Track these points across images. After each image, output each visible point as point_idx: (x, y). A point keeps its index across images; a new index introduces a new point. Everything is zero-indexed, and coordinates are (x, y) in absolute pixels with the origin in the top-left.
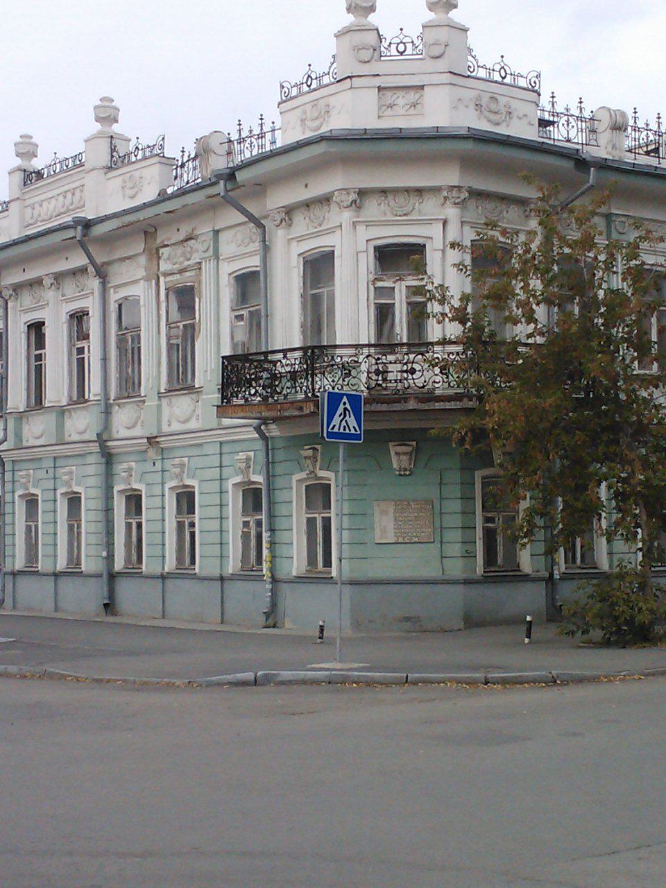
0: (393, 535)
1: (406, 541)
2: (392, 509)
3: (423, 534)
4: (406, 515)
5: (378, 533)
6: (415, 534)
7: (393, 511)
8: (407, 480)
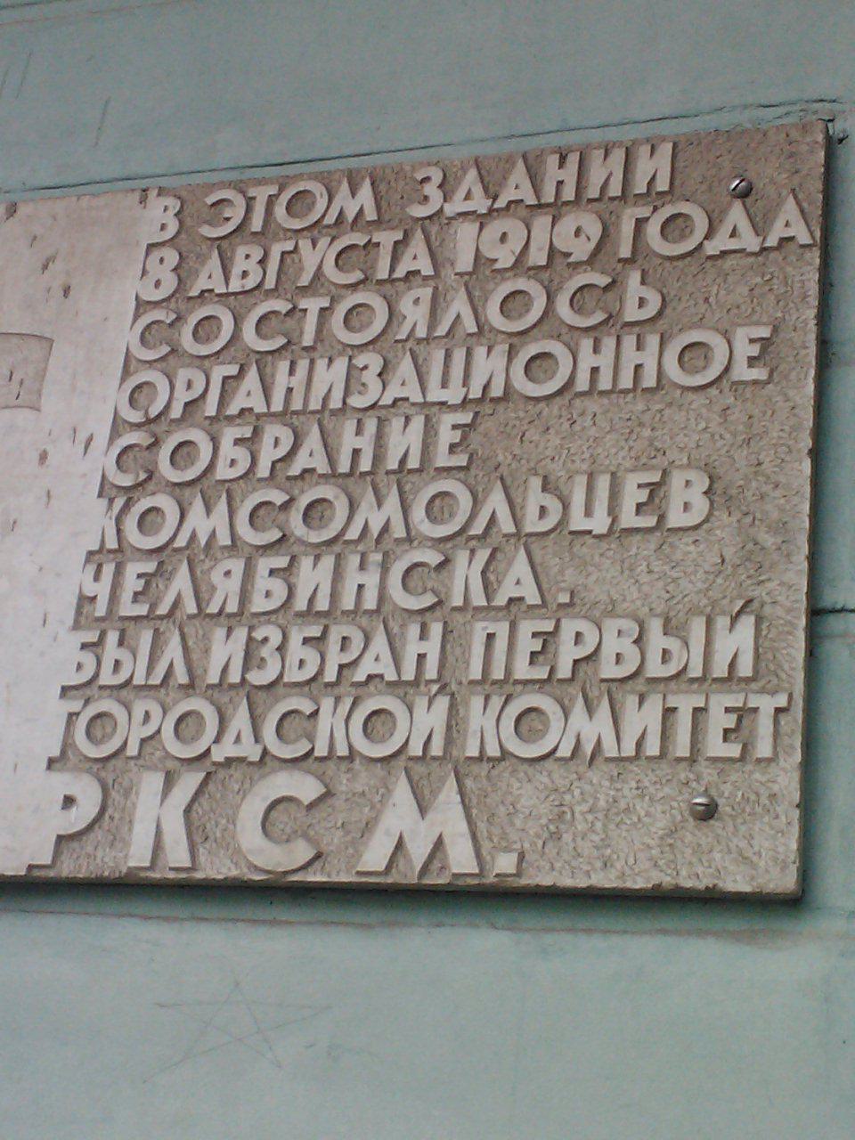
4: (330, 376)
7: (125, 336)
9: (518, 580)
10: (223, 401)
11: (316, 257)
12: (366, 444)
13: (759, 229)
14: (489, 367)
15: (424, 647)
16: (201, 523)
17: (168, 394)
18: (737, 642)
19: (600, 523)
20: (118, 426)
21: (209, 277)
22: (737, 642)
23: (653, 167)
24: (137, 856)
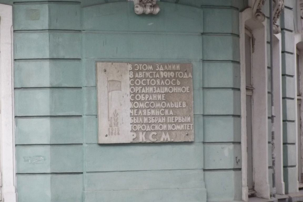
0: (129, 127)
1: (151, 139)
2: (128, 76)
3: (178, 127)
4: (151, 89)
5: (104, 123)
6: (164, 127)
7: (129, 82)
8: (150, 23)
9: (171, 113)
10: (141, 91)
11: (148, 74)
12: (156, 97)
13: (188, 76)
14: (166, 89)
15: (164, 119)
16: (142, 105)
17: (136, 90)
18: (189, 119)
19: (177, 107)
20: (131, 93)
21: (137, 76)
22: (189, 119)
23: (178, 67)
24: (140, 140)
